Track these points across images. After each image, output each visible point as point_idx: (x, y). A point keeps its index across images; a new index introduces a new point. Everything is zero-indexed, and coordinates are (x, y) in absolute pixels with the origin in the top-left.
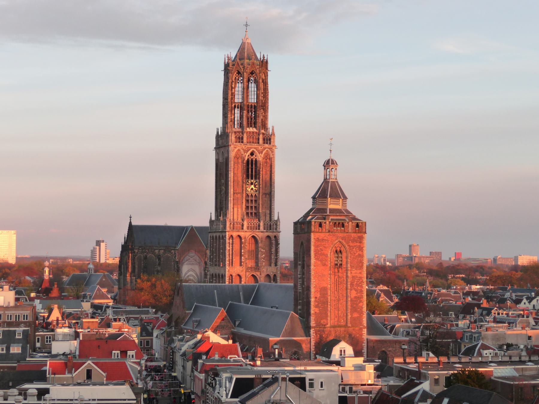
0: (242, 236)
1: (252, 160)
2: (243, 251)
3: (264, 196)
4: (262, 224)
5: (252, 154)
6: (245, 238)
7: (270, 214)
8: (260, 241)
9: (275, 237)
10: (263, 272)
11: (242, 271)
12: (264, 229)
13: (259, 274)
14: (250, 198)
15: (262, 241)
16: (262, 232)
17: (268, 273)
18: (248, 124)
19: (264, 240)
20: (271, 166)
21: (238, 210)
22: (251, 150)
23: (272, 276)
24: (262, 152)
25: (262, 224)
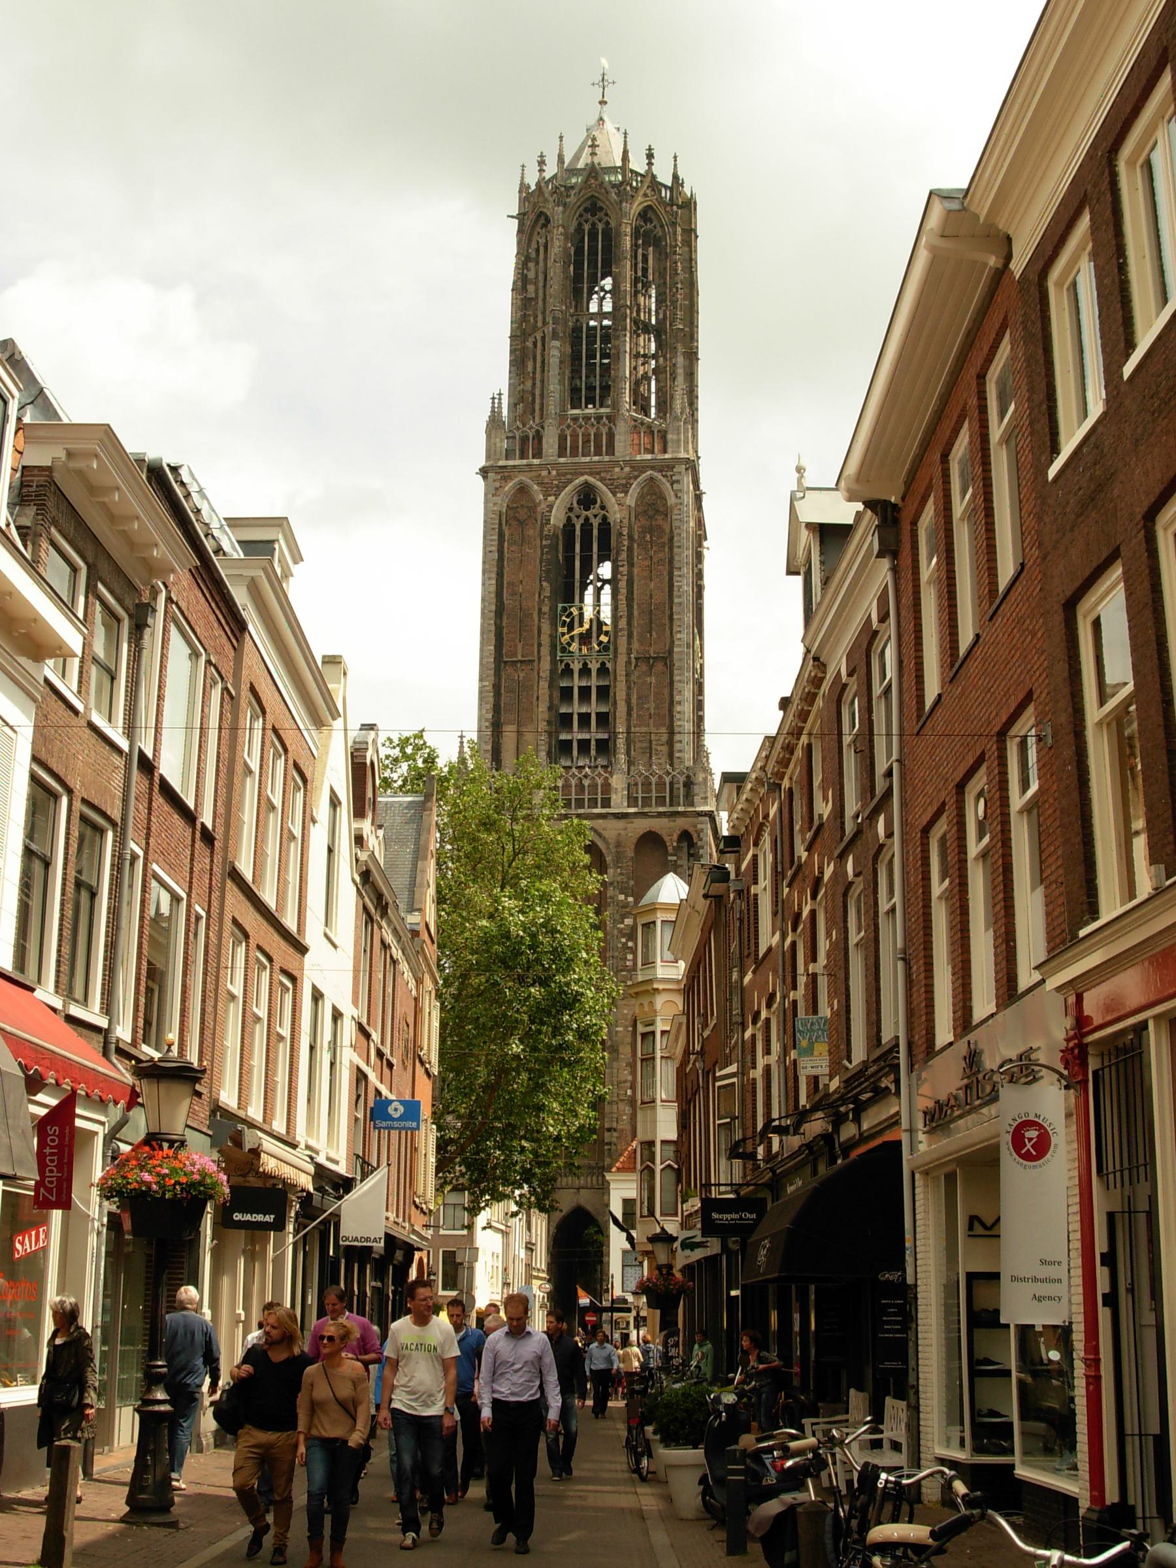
1: (587, 526)
3: (644, 667)
4: (618, 782)
5: (587, 497)
7: (670, 743)
8: (608, 859)
9: (686, 837)
12: (632, 800)
14: (577, 682)
15: (618, 858)
18: (575, 391)
19: (630, 853)
20: (671, 539)
22: (582, 479)
24: (625, 489)
25: (618, 782)
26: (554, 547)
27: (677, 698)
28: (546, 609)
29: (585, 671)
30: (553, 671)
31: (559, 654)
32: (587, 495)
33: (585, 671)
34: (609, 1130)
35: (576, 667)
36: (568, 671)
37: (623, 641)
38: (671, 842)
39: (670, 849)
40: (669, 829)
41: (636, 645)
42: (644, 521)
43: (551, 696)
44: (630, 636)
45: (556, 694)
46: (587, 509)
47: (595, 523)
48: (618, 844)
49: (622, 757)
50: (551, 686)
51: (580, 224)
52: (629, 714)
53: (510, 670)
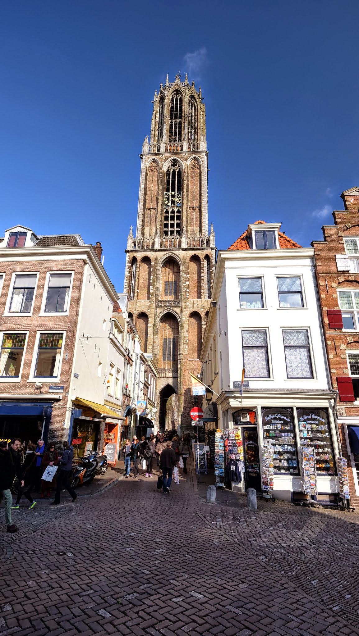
0: (151, 257)
1: (174, 171)
2: (152, 277)
3: (192, 210)
4: (184, 240)
5: (175, 163)
6: (156, 259)
7: (201, 231)
8: (180, 263)
9: (207, 257)
10: (186, 307)
11: (149, 307)
13: (178, 310)
16: (183, 250)
17: (194, 310)
21: (150, 230)
22: (172, 158)
23: (203, 314)
24: (186, 160)
26: (163, 176)
27: (203, 217)
28: (160, 193)
29: (173, 212)
30: (162, 210)
31: (164, 206)
32: (174, 163)
33: (173, 212)
34: (180, 354)
35: (170, 210)
36: (167, 212)
37: (185, 202)
38: (202, 258)
39: (202, 260)
40: (201, 254)
41: (189, 204)
42: (192, 170)
43: (161, 218)
44: (187, 200)
45: (163, 218)
46: (174, 167)
47: (177, 170)
48: (184, 259)
49: (185, 233)
50: (161, 214)
51: (173, 98)
52: (187, 221)
53: (148, 210)
